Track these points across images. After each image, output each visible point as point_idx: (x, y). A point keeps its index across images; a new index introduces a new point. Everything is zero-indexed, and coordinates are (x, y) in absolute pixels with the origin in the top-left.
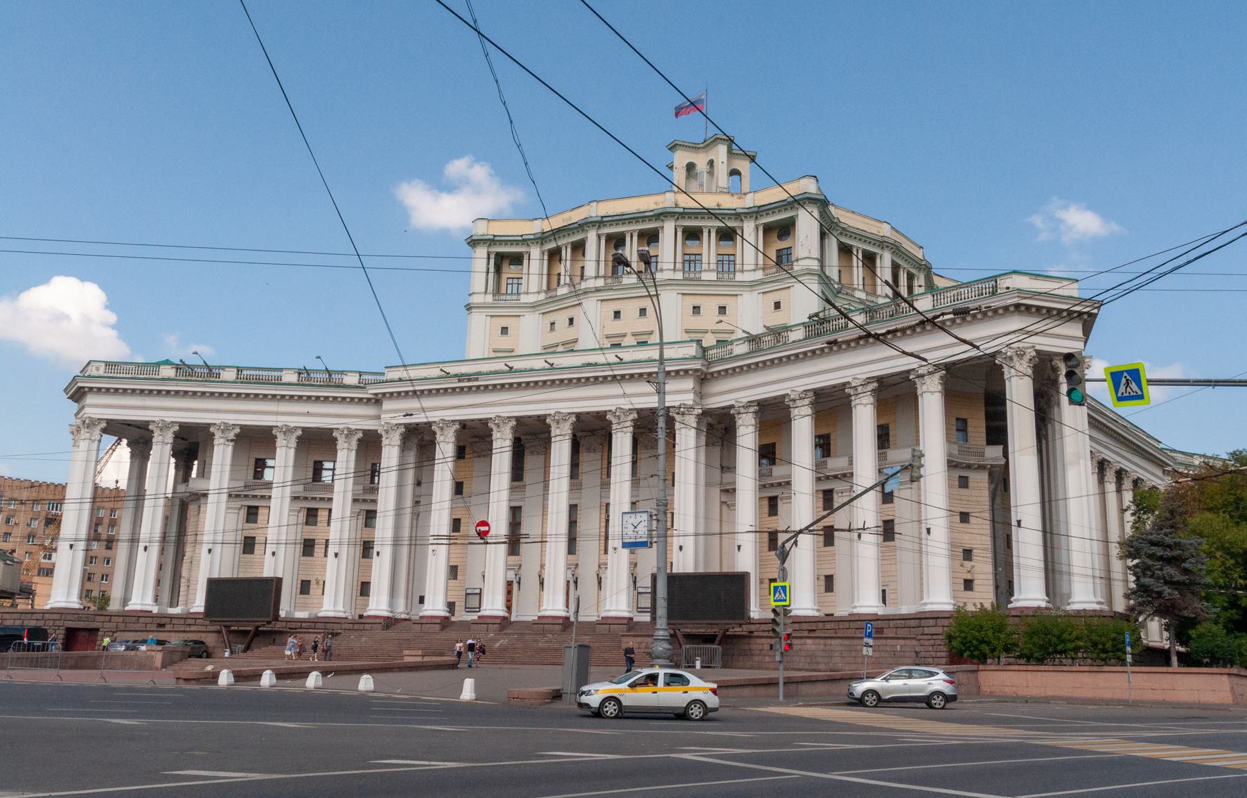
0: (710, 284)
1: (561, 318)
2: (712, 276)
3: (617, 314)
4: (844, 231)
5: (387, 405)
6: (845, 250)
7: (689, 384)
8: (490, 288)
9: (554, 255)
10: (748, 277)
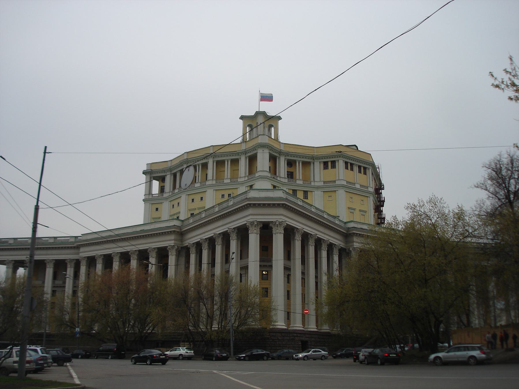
0: (227, 184)
1: (175, 203)
2: (229, 181)
3: (193, 200)
4: (287, 154)
5: (82, 249)
6: (290, 164)
7: (172, 237)
8: (215, 178)
9: (175, 176)
10: (243, 180)
